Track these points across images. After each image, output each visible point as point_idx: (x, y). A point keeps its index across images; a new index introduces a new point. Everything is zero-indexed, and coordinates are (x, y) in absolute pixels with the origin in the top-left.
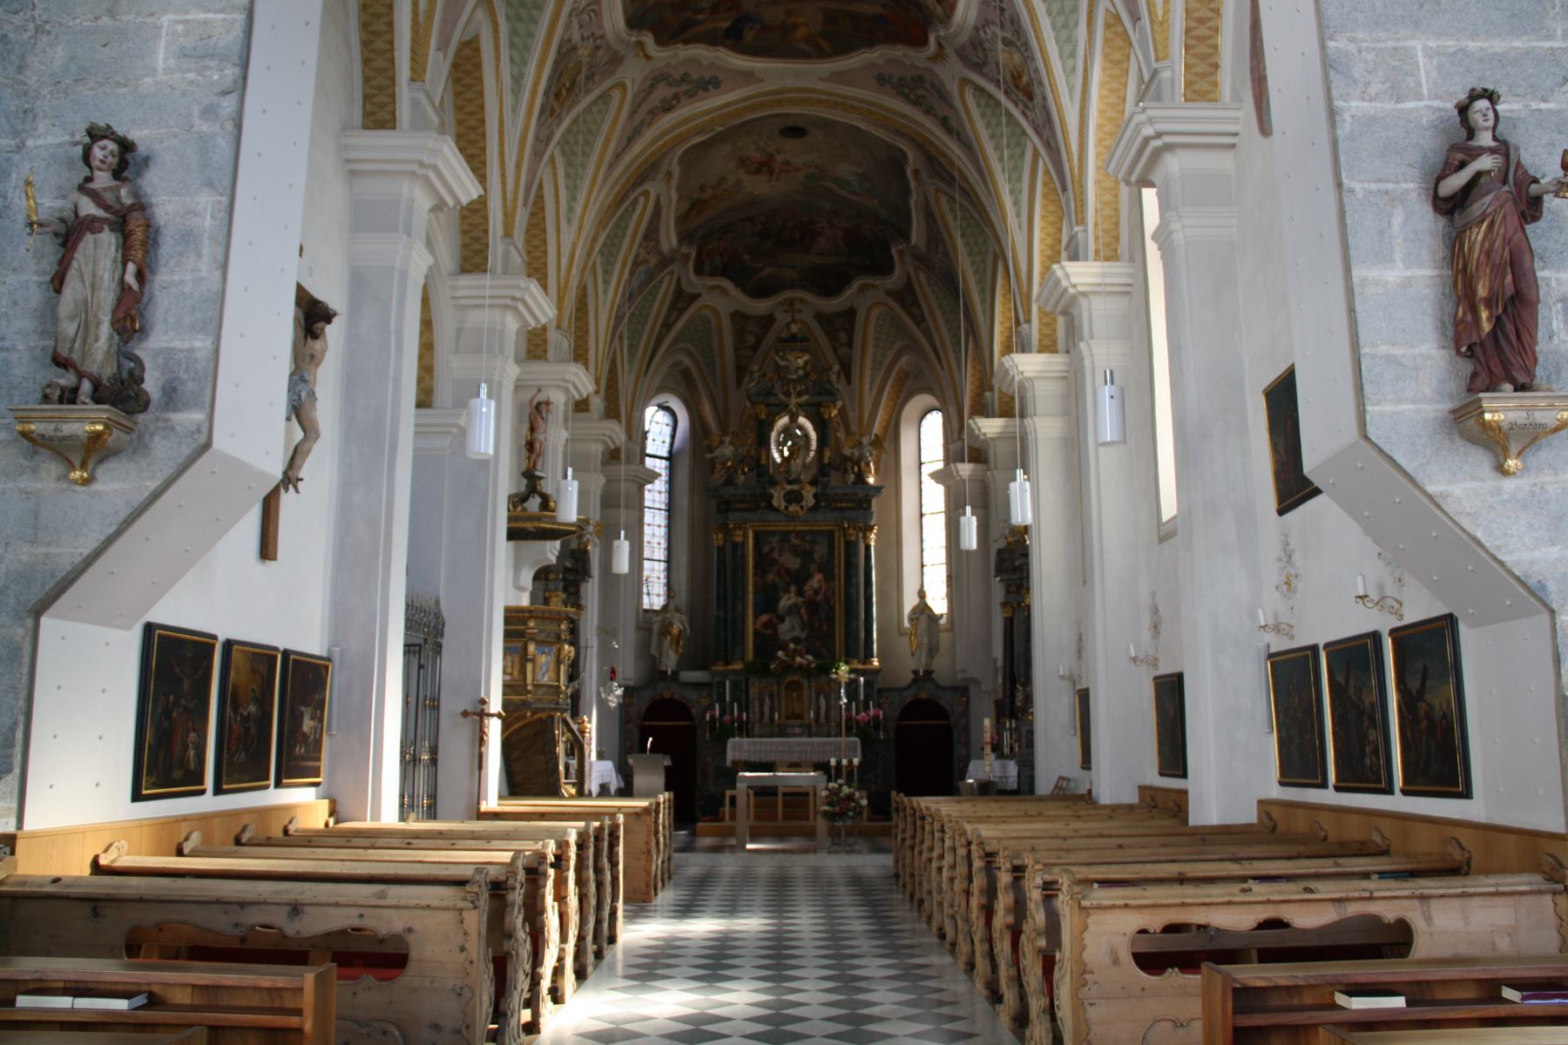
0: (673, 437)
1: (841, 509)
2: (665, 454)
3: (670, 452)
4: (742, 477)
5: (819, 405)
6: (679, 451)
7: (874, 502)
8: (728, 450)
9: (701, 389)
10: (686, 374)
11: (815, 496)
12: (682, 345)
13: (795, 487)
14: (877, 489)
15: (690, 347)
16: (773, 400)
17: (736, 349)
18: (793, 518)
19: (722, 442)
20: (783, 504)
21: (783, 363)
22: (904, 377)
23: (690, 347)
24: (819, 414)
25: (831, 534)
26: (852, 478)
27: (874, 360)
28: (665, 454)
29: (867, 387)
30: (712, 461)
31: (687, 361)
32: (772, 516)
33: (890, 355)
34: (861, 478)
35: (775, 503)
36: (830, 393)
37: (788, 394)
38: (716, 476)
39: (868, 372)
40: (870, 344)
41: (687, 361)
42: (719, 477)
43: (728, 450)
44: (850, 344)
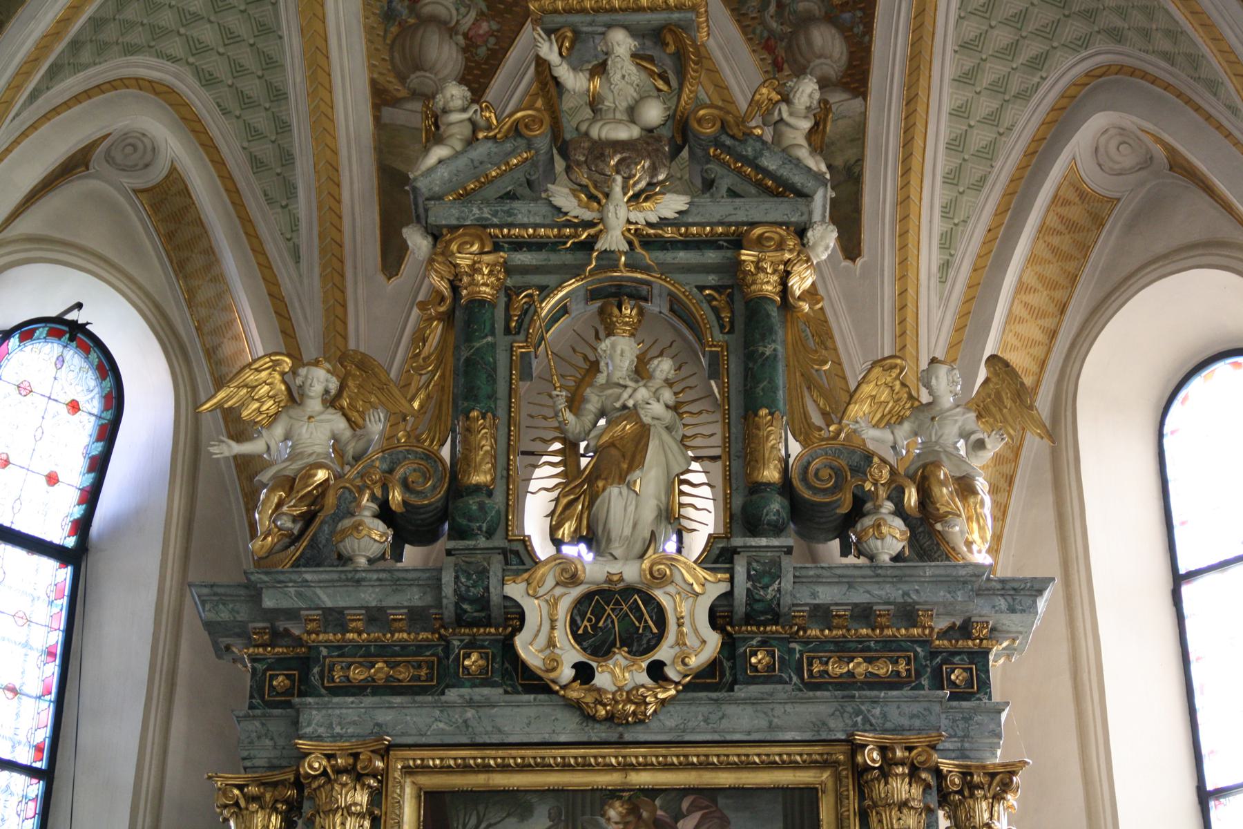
0: (99, 465)
1: (847, 683)
2: (62, 536)
3: (82, 527)
4: (377, 534)
5: (738, 243)
6: (122, 526)
7: (997, 664)
8: (319, 431)
9: (231, 263)
10: (169, 206)
11: (719, 616)
12: (145, 67)
13: (631, 572)
14: (1021, 593)
15: (188, 87)
16: (527, 217)
17: (381, 97)
18: (615, 725)
19: (294, 397)
20: (570, 654)
21: (574, 80)
22: (1085, 217)
23: (188, 87)
24: (734, 281)
25: (809, 795)
26: (892, 538)
27: (956, 145)
28: (62, 536)
29: (928, 257)
30: (247, 467)
31: (173, 146)
32: (520, 718)
33: (1027, 121)
34: (927, 533)
35: (529, 649)
36: (783, 189)
37: (596, 195)
38: (262, 518)
39: (931, 195)
40: (944, 66)
41: (173, 146)
42: (272, 516)
43: (319, 431)
44: (855, 78)
